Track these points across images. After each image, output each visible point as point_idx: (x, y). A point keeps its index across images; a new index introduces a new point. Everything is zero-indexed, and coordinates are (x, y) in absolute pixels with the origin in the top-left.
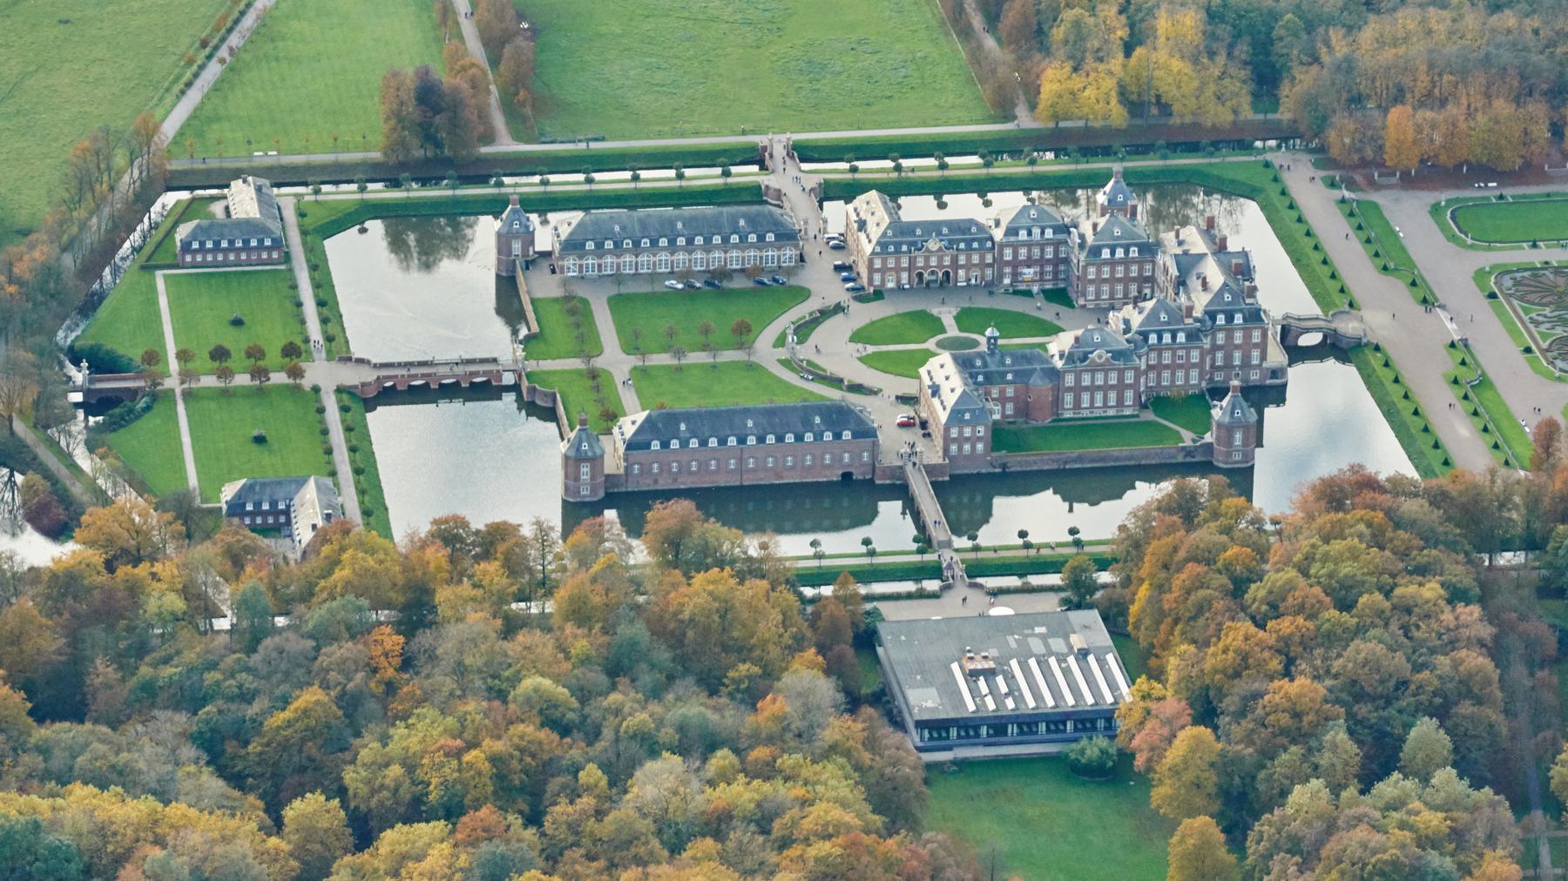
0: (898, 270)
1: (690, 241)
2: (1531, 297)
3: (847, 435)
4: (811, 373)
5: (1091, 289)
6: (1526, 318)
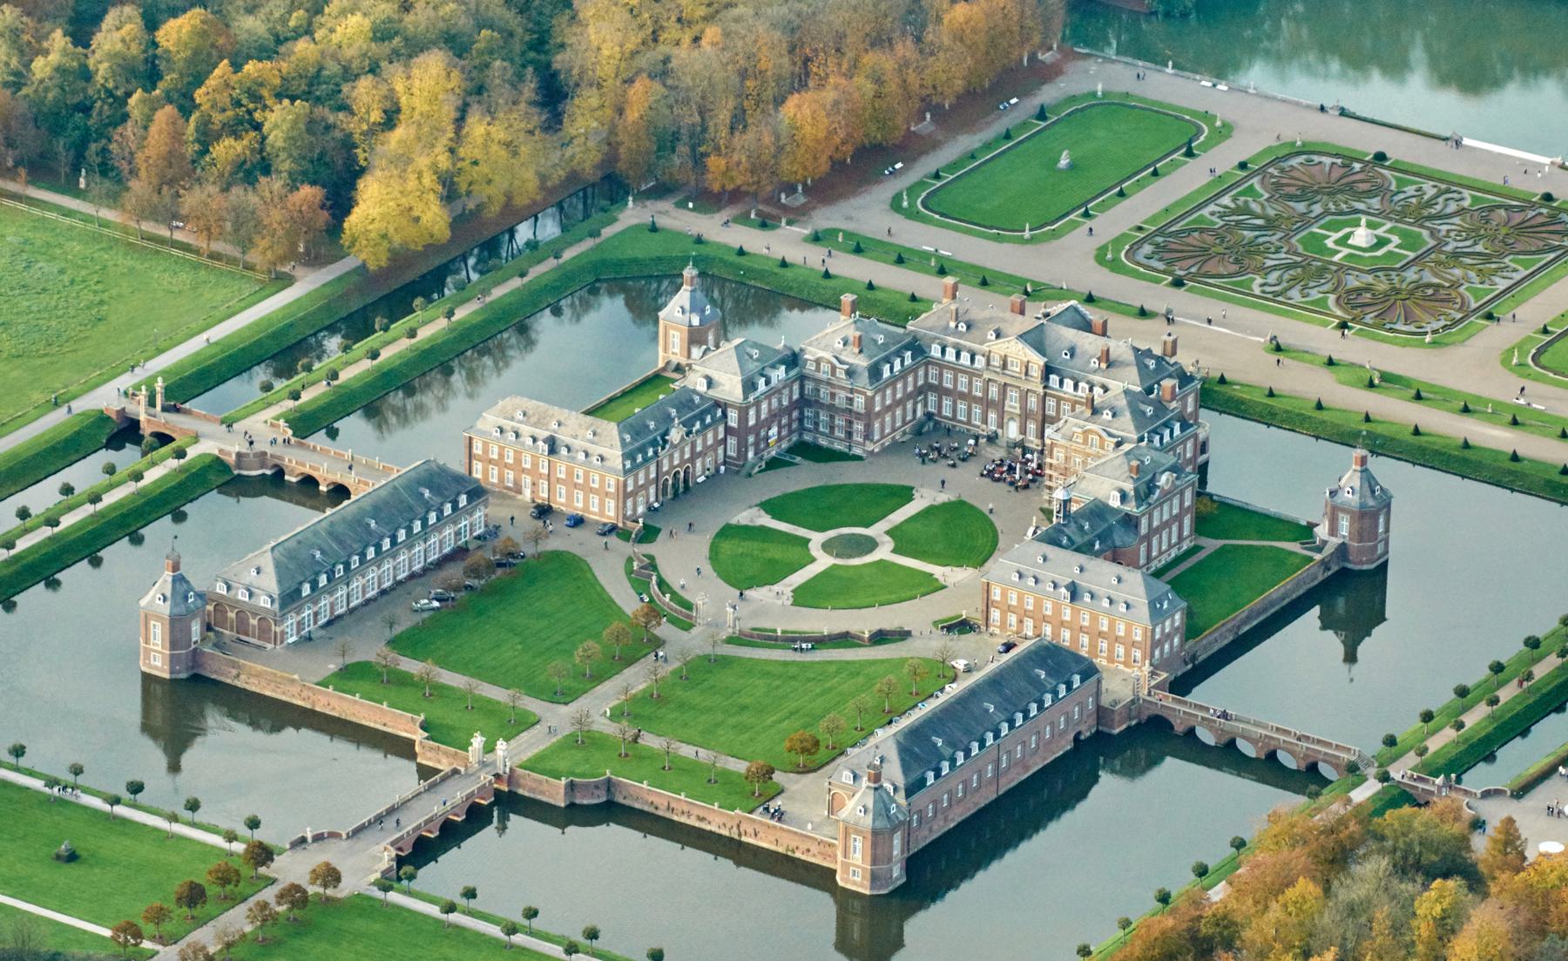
0: (645, 487)
1: (394, 543)
2: (1211, 267)
3: (1077, 678)
4: (806, 640)
5: (877, 425)
6: (1257, 291)
